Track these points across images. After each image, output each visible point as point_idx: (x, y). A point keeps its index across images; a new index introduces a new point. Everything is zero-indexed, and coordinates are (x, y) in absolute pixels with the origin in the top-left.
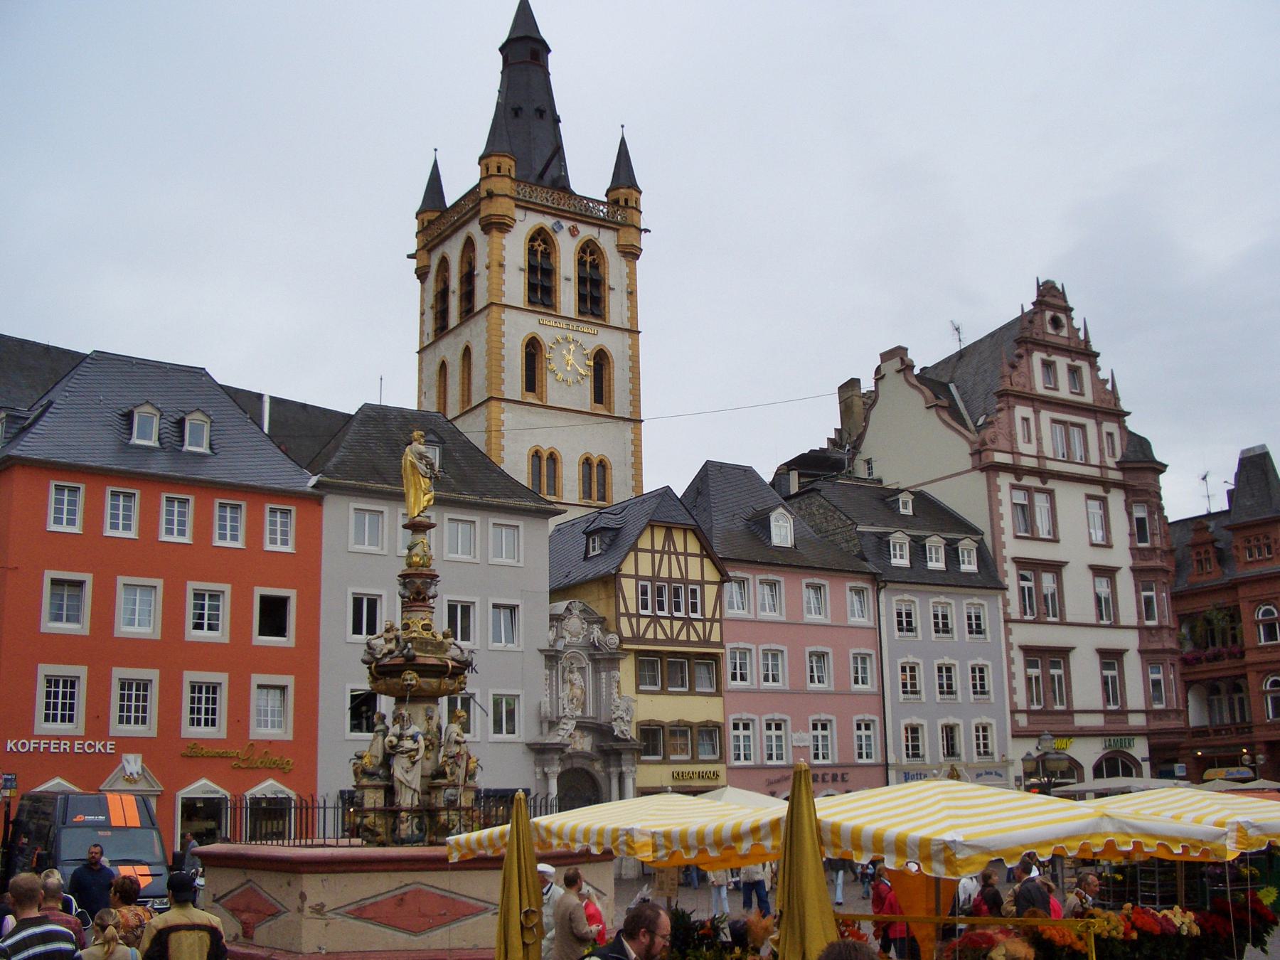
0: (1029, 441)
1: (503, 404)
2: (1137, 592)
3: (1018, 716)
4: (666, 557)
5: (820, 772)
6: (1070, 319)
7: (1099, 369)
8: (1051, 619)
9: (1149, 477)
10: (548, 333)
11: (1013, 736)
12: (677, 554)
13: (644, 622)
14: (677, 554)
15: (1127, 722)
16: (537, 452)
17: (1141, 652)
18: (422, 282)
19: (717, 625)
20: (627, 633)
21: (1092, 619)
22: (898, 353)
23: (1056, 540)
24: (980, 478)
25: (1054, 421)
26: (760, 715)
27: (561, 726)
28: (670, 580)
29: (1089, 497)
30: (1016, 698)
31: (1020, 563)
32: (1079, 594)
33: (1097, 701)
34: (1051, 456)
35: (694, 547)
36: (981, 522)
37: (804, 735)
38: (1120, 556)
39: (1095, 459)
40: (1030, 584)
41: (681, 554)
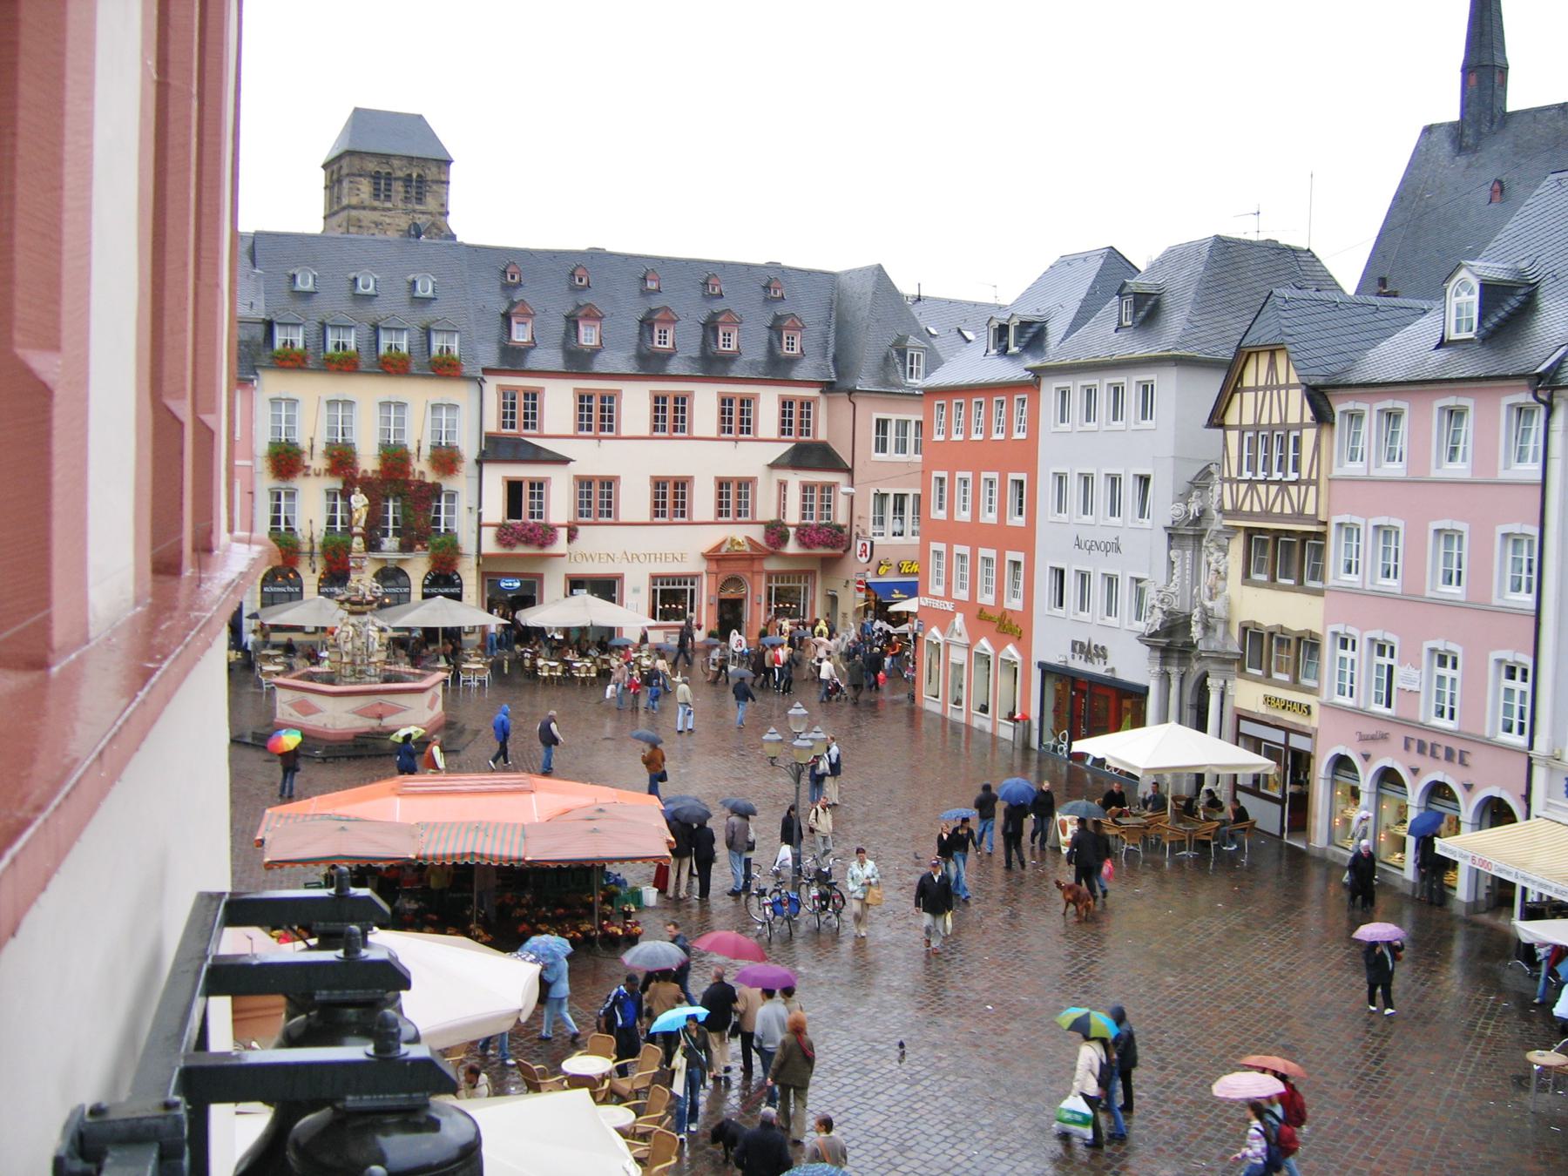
19: (1312, 489)
26: (1363, 630)
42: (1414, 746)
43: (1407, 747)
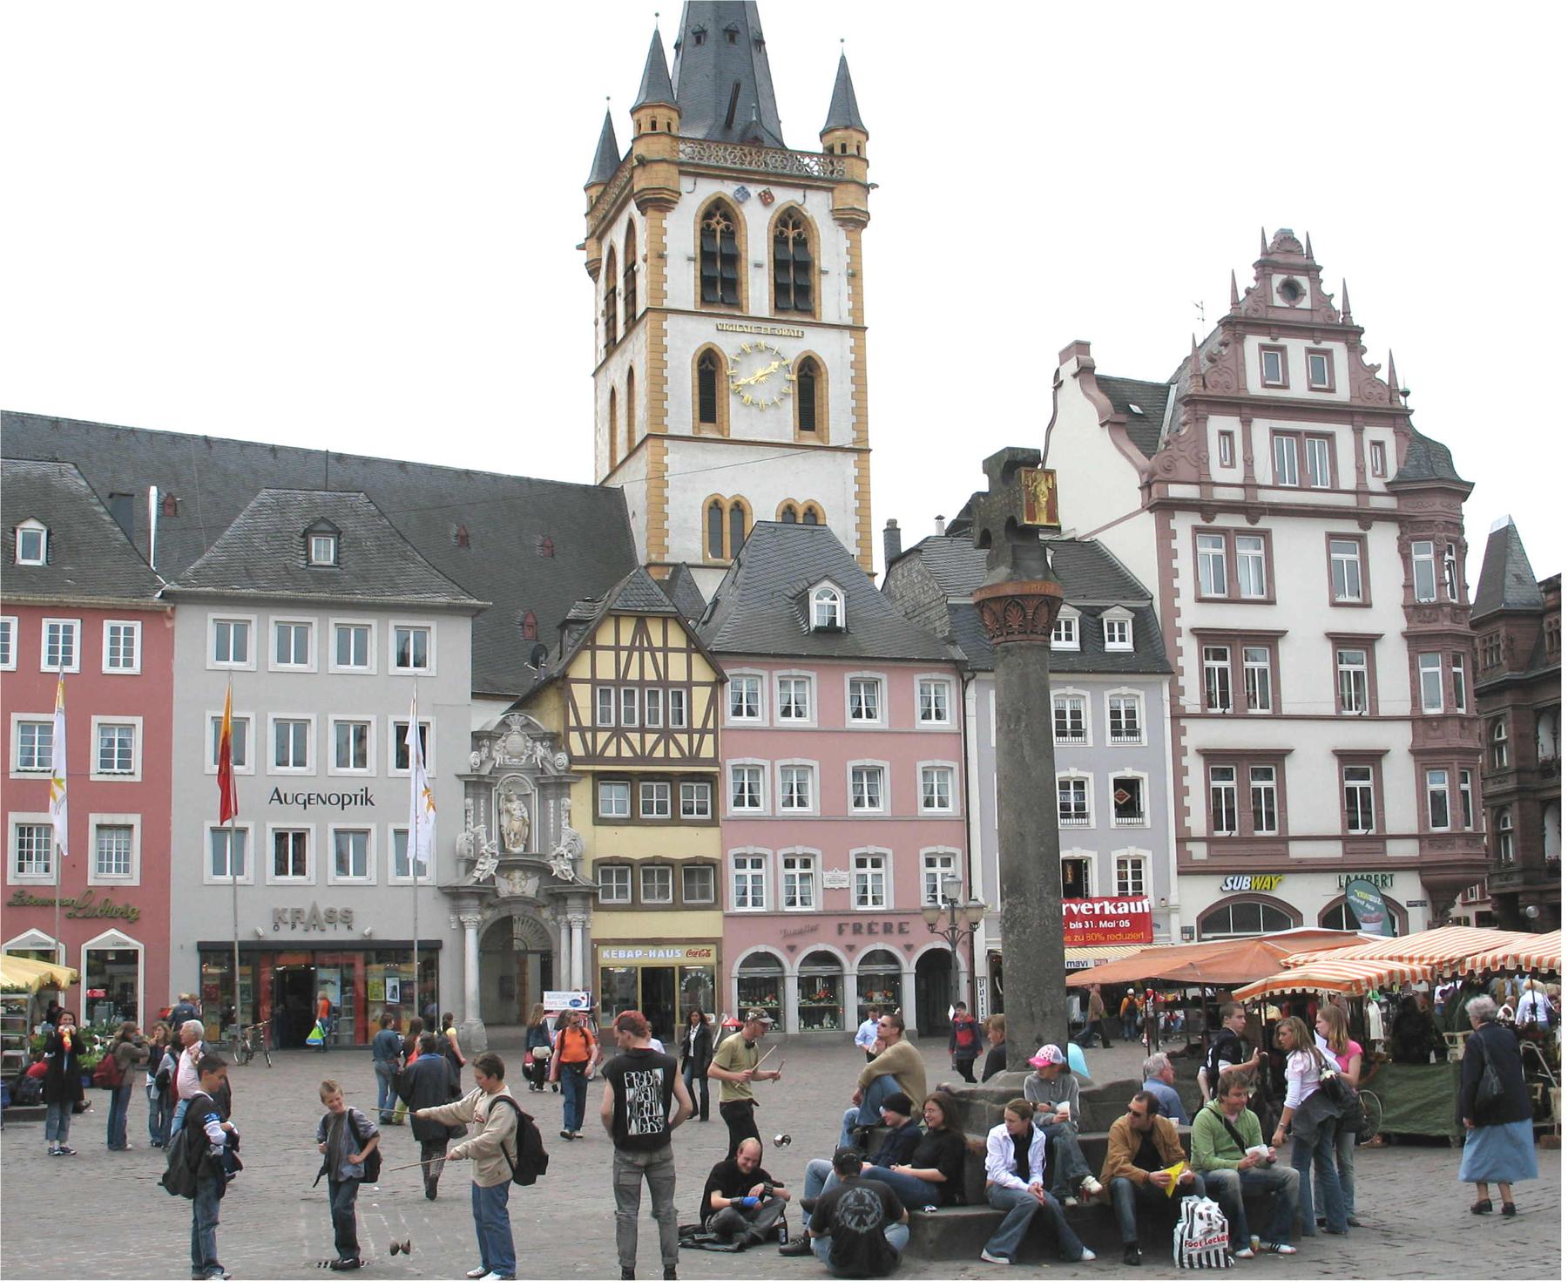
0: (1232, 465)
1: (667, 443)
2: (1413, 668)
3: (1190, 846)
4: (636, 655)
5: (865, 922)
6: (1316, 282)
7: (1364, 350)
8: (1258, 711)
9: (1436, 506)
10: (729, 344)
11: (1179, 873)
12: (653, 650)
13: (602, 738)
14: (653, 650)
15: (1287, 853)
16: (716, 502)
17: (1414, 752)
18: (596, 281)
19: (709, 738)
20: (578, 749)
21: (1331, 711)
22: (1081, 347)
23: (1271, 602)
24: (1149, 521)
25: (1275, 432)
27: (479, 866)
28: (642, 683)
29: (1331, 536)
30: (1188, 822)
31: (1202, 635)
32: (1306, 675)
33: (1330, 818)
34: (1269, 482)
35: (677, 639)
36: (1149, 580)
37: (843, 875)
38: (1386, 617)
39: (1348, 480)
40: (1225, 664)
41: (659, 649)
42: (848, 930)
43: (840, 931)
